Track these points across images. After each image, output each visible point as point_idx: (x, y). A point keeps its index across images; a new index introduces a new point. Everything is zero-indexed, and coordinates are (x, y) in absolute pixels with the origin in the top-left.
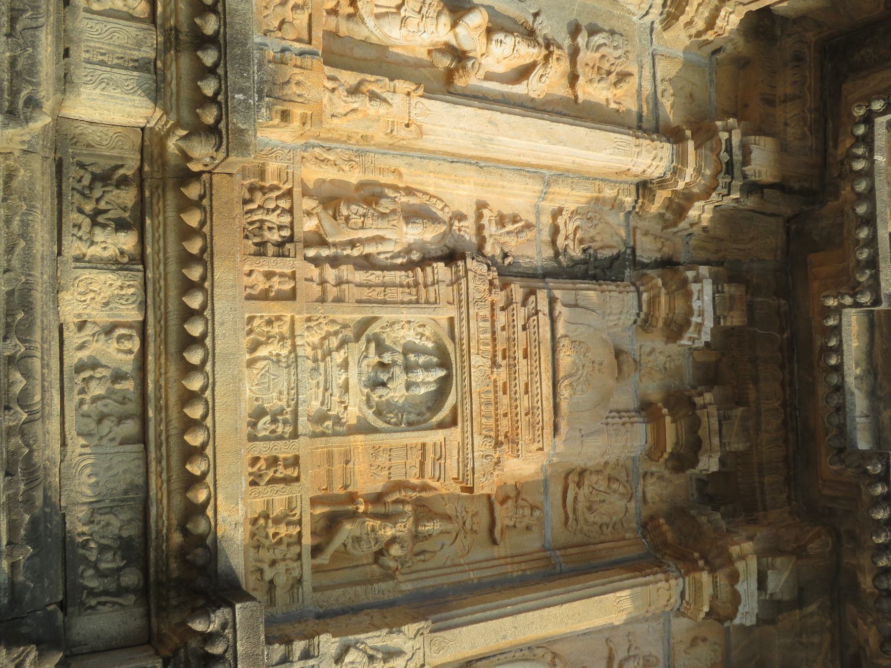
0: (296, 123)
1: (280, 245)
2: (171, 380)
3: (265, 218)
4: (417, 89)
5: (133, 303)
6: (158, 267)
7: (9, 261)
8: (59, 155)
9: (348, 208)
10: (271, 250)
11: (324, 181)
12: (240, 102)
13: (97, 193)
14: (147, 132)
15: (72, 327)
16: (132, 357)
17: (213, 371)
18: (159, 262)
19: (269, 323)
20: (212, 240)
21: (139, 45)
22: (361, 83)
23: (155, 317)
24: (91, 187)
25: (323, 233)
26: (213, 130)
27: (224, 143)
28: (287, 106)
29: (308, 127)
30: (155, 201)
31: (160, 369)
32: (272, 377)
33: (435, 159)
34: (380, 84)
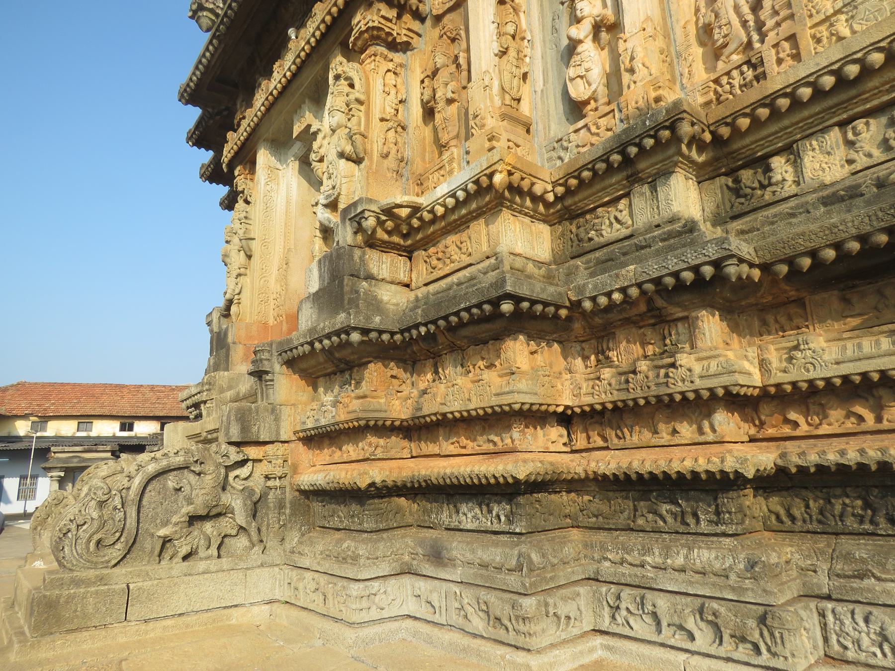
0: (660, 92)
1: (754, 67)
2: (882, 80)
3: (738, 86)
4: (621, 38)
5: (824, 137)
6: (790, 133)
7: (800, 213)
8: (728, 220)
9: (718, 40)
10: (760, 70)
11: (706, 69)
12: (651, 121)
13: (749, 191)
14: (700, 180)
15: (853, 166)
16: (871, 121)
17: (861, 50)
18: (786, 134)
19: (819, 41)
20: (754, 103)
21: (642, 194)
22: (627, 70)
23: (832, 118)
24: (745, 196)
25: (741, 48)
26: (672, 127)
27: (677, 117)
28: (652, 101)
29: (661, 84)
30: (743, 156)
31: (875, 94)
32: (867, 13)
33: (669, 7)
34: (624, 59)
